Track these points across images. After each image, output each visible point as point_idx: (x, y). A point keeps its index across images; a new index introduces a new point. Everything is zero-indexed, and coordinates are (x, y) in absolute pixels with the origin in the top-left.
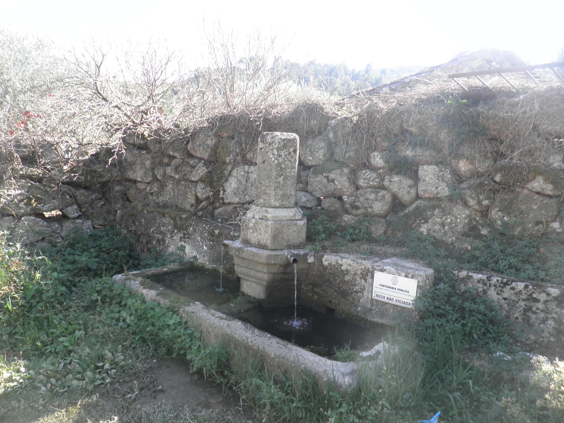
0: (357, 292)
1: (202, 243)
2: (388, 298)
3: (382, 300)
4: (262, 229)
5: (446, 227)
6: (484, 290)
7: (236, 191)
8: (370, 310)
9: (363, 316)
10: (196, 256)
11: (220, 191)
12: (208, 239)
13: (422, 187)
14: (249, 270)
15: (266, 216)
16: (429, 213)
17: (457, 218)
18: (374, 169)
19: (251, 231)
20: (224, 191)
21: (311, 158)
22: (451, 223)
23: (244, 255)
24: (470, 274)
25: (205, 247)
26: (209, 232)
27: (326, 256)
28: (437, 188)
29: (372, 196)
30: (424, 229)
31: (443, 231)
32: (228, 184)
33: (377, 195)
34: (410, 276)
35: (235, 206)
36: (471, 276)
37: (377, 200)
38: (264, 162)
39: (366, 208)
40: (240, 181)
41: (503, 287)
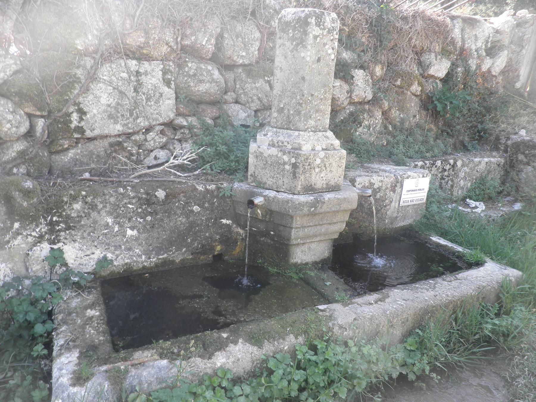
0: (385, 206)
1: (121, 225)
4: (334, 164)
7: (113, 111)
8: (397, 217)
9: (390, 226)
10: (105, 258)
11: (69, 115)
12: (138, 215)
14: (318, 227)
15: (332, 145)
16: (362, 117)
17: (376, 119)
19: (317, 170)
20: (82, 113)
21: (244, 54)
22: (373, 124)
23: (325, 208)
25: (129, 232)
26: (140, 199)
28: (365, 92)
32: (91, 97)
34: (425, 175)
35: (112, 140)
38: (319, 60)
40: (121, 92)
41: (432, 167)
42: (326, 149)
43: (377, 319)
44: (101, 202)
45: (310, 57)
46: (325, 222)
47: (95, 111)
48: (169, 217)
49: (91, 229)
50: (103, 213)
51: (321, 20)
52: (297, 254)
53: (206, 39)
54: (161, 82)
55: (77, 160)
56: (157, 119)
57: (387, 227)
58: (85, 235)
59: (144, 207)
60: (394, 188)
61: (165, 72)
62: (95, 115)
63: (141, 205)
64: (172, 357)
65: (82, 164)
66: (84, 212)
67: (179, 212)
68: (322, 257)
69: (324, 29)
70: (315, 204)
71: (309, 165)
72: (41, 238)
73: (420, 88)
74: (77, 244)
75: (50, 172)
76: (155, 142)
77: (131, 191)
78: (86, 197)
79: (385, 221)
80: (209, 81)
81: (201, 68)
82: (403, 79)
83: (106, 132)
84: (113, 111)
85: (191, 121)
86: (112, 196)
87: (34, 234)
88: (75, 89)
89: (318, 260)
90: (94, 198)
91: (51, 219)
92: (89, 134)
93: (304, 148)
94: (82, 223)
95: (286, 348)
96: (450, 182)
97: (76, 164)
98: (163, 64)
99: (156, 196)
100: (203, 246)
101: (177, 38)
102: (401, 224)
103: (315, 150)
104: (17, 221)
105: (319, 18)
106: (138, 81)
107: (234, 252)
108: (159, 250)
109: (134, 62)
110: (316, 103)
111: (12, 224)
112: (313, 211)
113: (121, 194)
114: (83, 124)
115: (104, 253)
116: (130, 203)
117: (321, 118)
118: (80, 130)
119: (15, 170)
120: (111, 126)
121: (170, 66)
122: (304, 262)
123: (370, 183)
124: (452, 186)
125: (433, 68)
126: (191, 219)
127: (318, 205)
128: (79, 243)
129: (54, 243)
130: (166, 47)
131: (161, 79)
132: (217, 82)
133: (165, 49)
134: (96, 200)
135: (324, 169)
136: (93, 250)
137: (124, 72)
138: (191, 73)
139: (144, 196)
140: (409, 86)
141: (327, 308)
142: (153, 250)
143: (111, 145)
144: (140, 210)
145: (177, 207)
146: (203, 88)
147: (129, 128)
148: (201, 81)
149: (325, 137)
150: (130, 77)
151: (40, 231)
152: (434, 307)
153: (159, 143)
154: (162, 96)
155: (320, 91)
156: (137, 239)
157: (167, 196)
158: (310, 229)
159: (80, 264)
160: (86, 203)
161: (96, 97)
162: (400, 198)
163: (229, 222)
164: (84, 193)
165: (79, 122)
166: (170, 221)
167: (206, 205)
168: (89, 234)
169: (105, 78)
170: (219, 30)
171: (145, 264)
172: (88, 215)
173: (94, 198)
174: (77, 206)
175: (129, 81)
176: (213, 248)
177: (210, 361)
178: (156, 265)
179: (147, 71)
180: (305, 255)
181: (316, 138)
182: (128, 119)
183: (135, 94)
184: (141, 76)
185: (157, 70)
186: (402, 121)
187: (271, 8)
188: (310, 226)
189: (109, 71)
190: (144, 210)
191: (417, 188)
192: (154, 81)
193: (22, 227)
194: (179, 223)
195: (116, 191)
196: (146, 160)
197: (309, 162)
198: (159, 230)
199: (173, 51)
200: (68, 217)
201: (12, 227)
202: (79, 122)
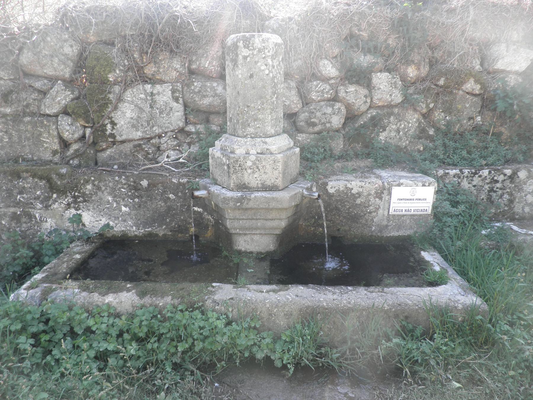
0: (370, 213)
1: (118, 203)
2: (406, 211)
3: (401, 213)
4: (268, 166)
5: (401, 133)
6: (459, 183)
7: (135, 122)
8: (387, 226)
9: (379, 234)
10: (108, 225)
11: (105, 126)
12: (129, 197)
13: (377, 96)
14: (254, 221)
15: (267, 149)
16: (386, 121)
17: (409, 123)
18: (326, 80)
19: (249, 171)
20: (113, 124)
22: (404, 128)
23: (251, 204)
24: (447, 171)
25: (124, 209)
26: (129, 185)
27: (330, 184)
28: (391, 95)
29: (329, 110)
30: (383, 136)
31: (398, 137)
32: (119, 113)
33: (333, 109)
34: (427, 184)
35: (136, 143)
36: (448, 173)
37: (334, 114)
38: (251, 76)
39: (324, 124)
40: (140, 108)
41: (473, 177)
42: (261, 154)
43: (252, 303)
44: (103, 186)
45: (242, 75)
46: (258, 217)
47: (122, 123)
48: (151, 200)
49: (99, 203)
50: (105, 193)
51: (249, 43)
52: (240, 242)
53: (208, 62)
54: (170, 99)
55: (111, 156)
56: (168, 127)
57: (374, 234)
58: (95, 206)
59: (132, 191)
60: (381, 195)
61: (173, 91)
62: (122, 125)
63: (131, 190)
64: (85, 289)
65: (115, 159)
66: (93, 192)
67: (159, 198)
68: (267, 249)
69: (254, 49)
70: (240, 200)
71: (240, 166)
72: (68, 206)
73: (479, 87)
74: (90, 212)
75: (96, 164)
76: (168, 144)
77: (124, 179)
78: (94, 181)
79: (371, 227)
80: (212, 96)
81: (206, 86)
82: (447, 79)
83: (131, 137)
84: (135, 122)
85: (199, 129)
86: (110, 182)
87: (64, 202)
88: (108, 108)
89: (263, 251)
90: (99, 182)
91: (74, 194)
92: (118, 138)
93: (238, 152)
94: (93, 198)
95: (160, 304)
96: (506, 196)
97: (110, 159)
98: (172, 86)
99: (141, 184)
100: (179, 226)
101: (185, 64)
102: (395, 234)
103: (249, 153)
104: (55, 193)
105: (246, 41)
106: (152, 99)
107: (206, 235)
108: (146, 224)
109: (149, 86)
110: (253, 113)
111: (52, 195)
112: (239, 206)
113: (116, 181)
114: (114, 131)
115: (108, 221)
116: (122, 188)
117: (261, 126)
118: (113, 136)
119: (71, 162)
120: (134, 133)
121: (177, 86)
122: (248, 251)
123: (347, 188)
124: (511, 201)
125: (500, 61)
126: (168, 204)
127: (243, 201)
128: (92, 212)
129: (78, 210)
130: (175, 72)
131: (171, 97)
132: (219, 96)
133: (174, 74)
134: (100, 184)
135: (257, 170)
136: (101, 218)
137: (141, 94)
138: (196, 90)
139: (132, 184)
140: (459, 85)
141: (218, 286)
142: (141, 224)
143: (135, 146)
144: (130, 194)
145: (157, 193)
146: (206, 101)
147: (148, 135)
148: (204, 96)
149: (263, 142)
150: (146, 97)
151: (68, 200)
152: (327, 309)
153: (171, 145)
154: (172, 109)
155: (257, 102)
156: (129, 214)
157: (149, 185)
158: (245, 221)
159: (93, 226)
160: (94, 185)
161: (123, 113)
162: (390, 206)
163: (200, 210)
164: (93, 178)
165: (112, 131)
166: (152, 203)
167: (180, 194)
168: (97, 207)
169: (128, 99)
170: (220, 53)
171: (136, 233)
172: (96, 193)
173: (99, 182)
174: (89, 187)
175: (146, 100)
176: (187, 230)
177: (103, 297)
178: (145, 236)
179: (159, 92)
180: (248, 244)
181: (253, 143)
182: (146, 127)
183: (150, 109)
184: (155, 95)
185: (167, 90)
186: (449, 124)
187: (270, 28)
188: (243, 219)
189: (131, 94)
190: (133, 194)
191: (415, 197)
192: (165, 98)
193: (58, 197)
194: (159, 206)
195: (113, 179)
196: (159, 158)
197: (240, 164)
198: (145, 209)
199: (181, 74)
200: (84, 193)
201: (52, 197)
202: (112, 131)
